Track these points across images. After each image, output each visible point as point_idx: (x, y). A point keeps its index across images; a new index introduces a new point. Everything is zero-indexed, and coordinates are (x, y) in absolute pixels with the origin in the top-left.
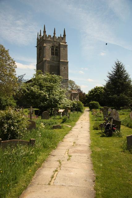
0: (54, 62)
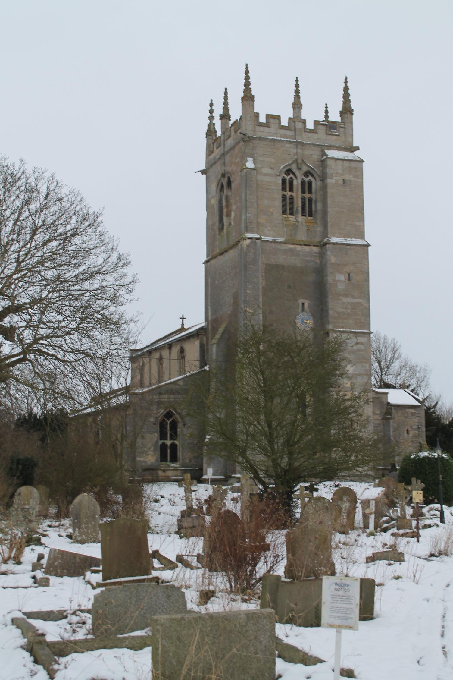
0: (299, 248)
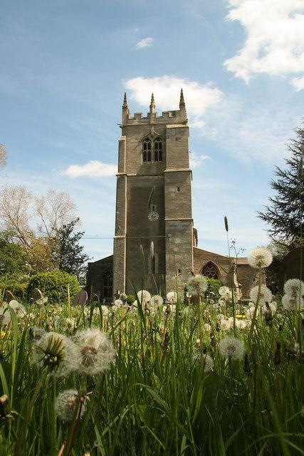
0: (151, 177)
